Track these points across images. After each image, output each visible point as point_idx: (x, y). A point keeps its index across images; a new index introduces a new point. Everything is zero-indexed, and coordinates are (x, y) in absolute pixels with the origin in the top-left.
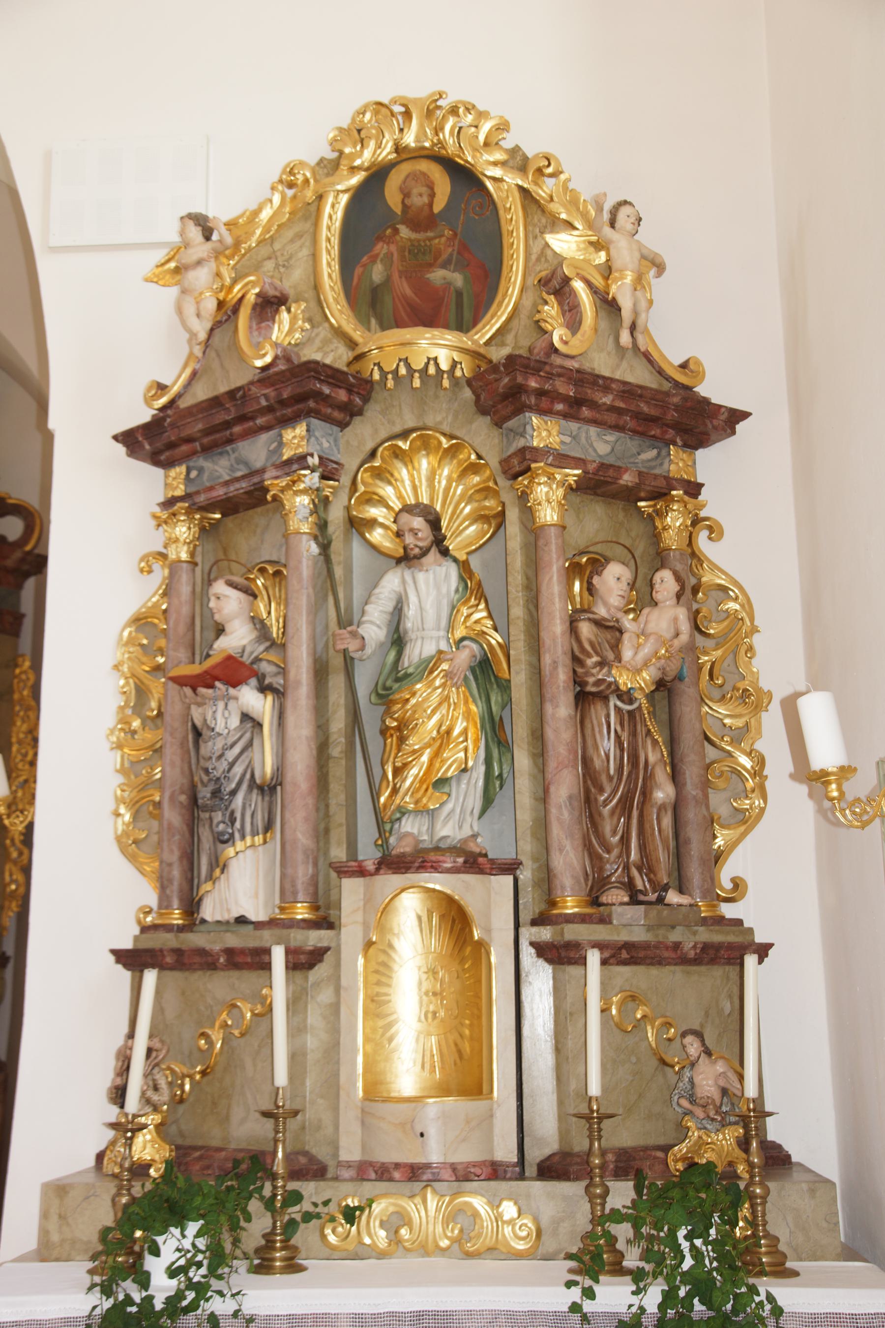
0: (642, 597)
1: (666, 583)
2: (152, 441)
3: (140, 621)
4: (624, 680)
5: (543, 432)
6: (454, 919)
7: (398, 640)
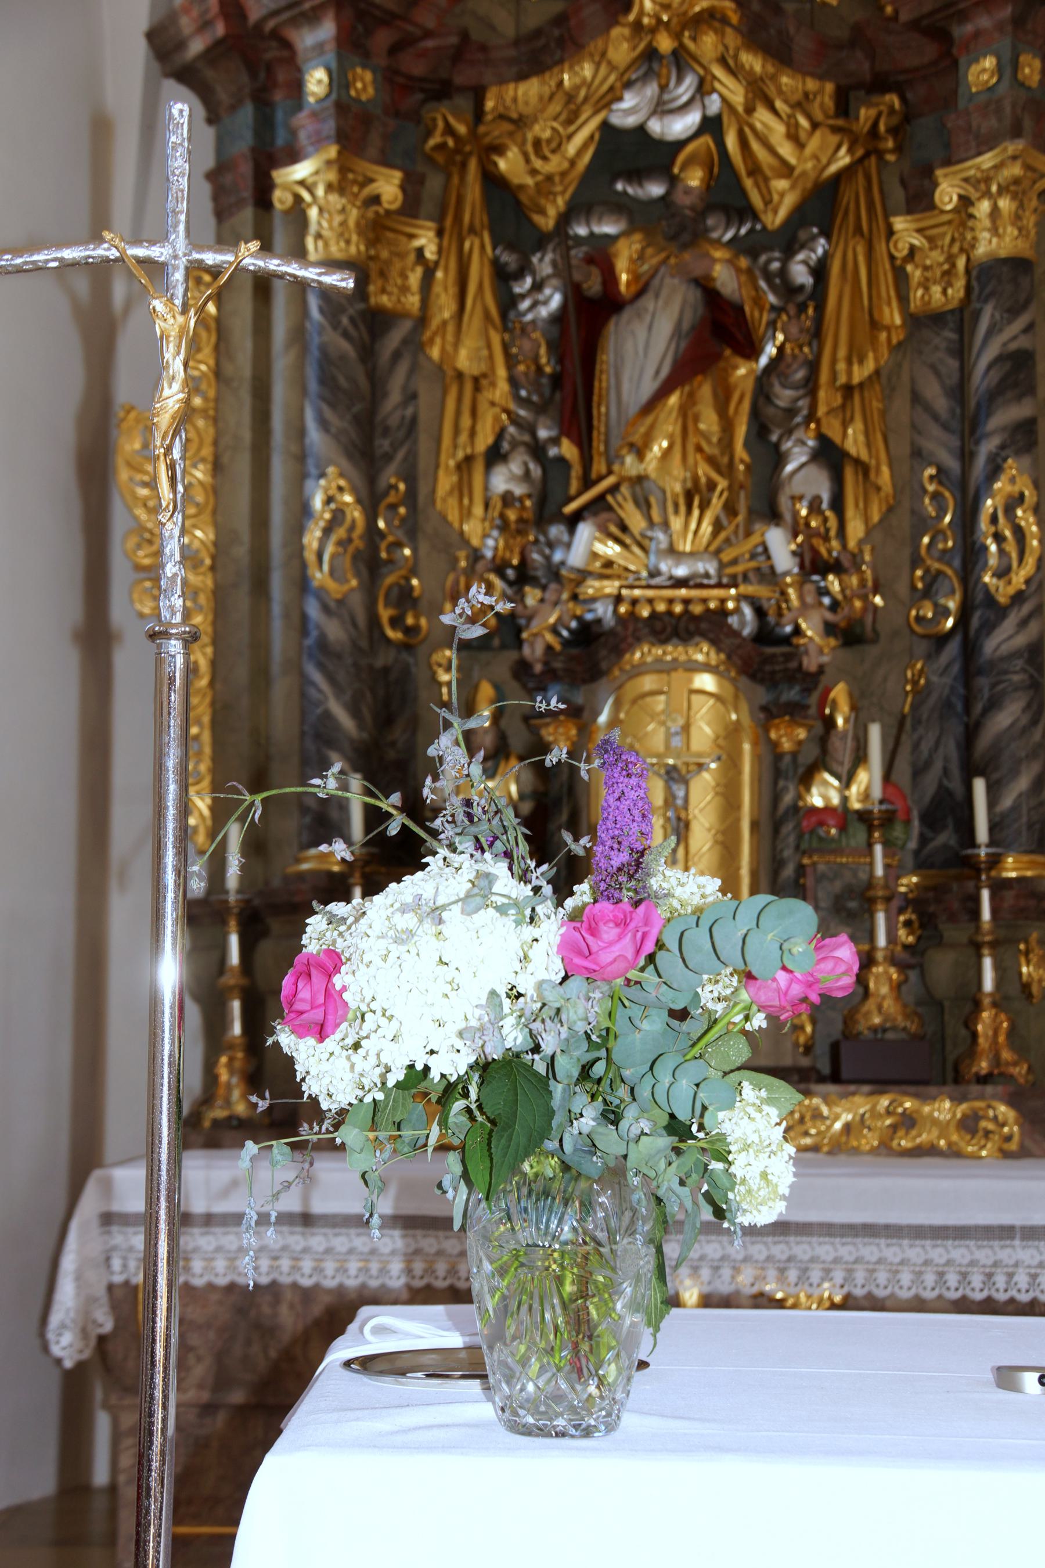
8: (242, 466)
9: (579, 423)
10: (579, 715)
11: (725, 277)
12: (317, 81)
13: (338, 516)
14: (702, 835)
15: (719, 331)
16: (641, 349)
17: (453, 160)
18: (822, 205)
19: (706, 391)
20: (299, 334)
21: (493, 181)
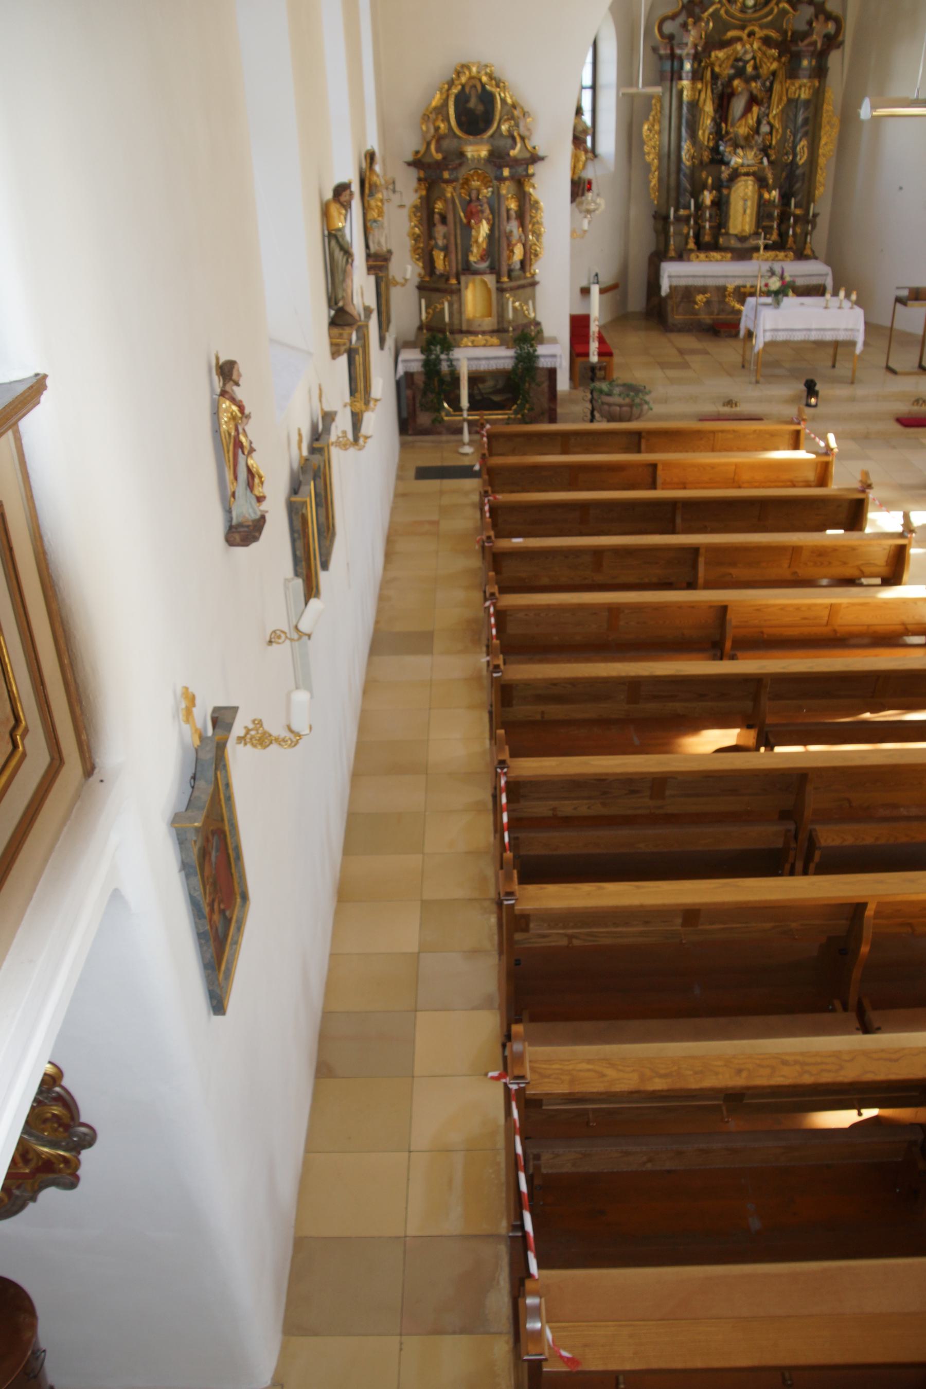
10: (729, 188)
11: (755, 92)
13: (689, 150)
15: (753, 100)
16: (738, 105)
17: (706, 68)
19: (749, 115)
21: (713, 71)
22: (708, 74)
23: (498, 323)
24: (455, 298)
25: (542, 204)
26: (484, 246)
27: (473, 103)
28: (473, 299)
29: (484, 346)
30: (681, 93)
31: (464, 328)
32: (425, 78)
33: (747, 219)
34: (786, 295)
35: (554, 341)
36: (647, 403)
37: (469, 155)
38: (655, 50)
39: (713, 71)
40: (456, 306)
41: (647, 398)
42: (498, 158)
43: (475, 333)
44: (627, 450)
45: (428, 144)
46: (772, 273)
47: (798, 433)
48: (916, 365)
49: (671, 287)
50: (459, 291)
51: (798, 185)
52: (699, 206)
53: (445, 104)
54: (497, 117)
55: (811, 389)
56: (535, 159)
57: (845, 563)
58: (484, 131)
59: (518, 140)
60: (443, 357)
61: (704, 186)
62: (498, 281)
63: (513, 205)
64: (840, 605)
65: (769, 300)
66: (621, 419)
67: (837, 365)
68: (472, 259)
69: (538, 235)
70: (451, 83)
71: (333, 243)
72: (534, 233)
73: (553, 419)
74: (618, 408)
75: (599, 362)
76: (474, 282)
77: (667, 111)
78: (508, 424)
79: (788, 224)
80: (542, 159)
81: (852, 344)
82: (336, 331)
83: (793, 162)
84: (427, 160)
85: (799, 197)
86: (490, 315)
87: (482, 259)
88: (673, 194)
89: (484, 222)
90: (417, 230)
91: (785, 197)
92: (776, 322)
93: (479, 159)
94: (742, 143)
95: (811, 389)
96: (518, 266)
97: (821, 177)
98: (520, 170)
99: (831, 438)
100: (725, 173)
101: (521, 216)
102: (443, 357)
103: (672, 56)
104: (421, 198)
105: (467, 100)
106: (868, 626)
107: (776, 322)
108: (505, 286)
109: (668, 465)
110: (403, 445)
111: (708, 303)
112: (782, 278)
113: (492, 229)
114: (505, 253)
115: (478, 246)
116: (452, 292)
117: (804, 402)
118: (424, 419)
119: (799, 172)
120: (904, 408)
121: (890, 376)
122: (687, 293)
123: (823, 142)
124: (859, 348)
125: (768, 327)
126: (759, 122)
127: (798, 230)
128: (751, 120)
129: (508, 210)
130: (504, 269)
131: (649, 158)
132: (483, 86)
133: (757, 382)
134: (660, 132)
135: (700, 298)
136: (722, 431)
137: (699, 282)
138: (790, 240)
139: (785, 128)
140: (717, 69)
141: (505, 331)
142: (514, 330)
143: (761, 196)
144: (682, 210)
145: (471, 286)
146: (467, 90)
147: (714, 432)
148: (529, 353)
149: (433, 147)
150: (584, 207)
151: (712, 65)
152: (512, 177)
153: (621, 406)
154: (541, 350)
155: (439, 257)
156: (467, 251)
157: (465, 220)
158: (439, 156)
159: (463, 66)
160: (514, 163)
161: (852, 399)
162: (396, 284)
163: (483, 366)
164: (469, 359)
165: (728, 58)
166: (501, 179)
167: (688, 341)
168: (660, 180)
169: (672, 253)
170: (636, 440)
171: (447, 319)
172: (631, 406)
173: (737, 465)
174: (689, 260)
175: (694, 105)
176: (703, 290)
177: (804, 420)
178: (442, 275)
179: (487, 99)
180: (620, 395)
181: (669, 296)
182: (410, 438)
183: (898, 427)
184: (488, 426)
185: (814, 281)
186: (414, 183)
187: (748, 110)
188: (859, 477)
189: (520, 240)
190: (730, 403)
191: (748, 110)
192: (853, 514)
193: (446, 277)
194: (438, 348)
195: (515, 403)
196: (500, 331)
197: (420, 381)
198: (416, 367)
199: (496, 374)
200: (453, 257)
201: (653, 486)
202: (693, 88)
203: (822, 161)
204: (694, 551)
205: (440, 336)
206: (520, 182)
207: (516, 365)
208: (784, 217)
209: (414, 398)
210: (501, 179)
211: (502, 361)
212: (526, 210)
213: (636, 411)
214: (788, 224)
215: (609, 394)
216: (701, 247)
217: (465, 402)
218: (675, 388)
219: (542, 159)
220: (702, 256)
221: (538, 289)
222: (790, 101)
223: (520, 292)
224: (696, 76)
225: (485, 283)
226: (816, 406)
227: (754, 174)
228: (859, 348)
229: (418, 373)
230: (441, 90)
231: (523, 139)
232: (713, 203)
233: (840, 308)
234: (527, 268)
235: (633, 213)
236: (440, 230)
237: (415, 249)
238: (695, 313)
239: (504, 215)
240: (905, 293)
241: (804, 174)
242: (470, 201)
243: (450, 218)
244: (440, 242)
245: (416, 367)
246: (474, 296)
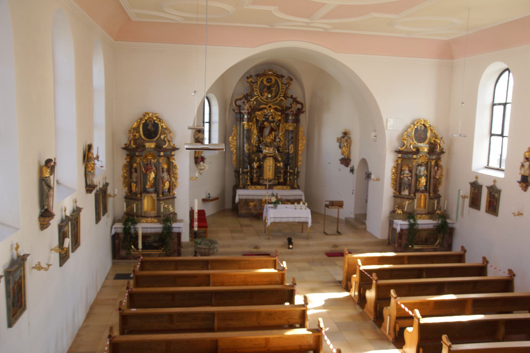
0: (438, 169)
1: (440, 169)
2: (398, 152)
3: (395, 167)
4: (437, 177)
5: (434, 157)
6: (425, 196)
7: (420, 172)
8: (238, 140)
9: (262, 136)
10: (263, 161)
11: (273, 127)
12: (246, 117)
14: (271, 170)
15: (272, 130)
16: (267, 131)
17: (253, 117)
18: (280, 120)
20: (244, 134)
21: (256, 119)
22: (255, 120)
23: (158, 213)
24: (139, 202)
25: (178, 167)
26: (152, 182)
27: (150, 127)
28: (147, 203)
29: (151, 223)
30: (244, 125)
31: (143, 215)
32: (130, 117)
33: (271, 173)
34: (279, 204)
35: (181, 221)
36: (215, 248)
37: (147, 146)
38: (234, 110)
39: (256, 119)
40: (139, 206)
41: (216, 246)
42: (159, 148)
43: (147, 217)
44: (203, 269)
45: (130, 141)
46: (273, 195)
47: (275, 260)
48: (336, 231)
49: (239, 199)
50: (141, 200)
51: (290, 161)
52: (252, 168)
53: (138, 126)
54: (159, 133)
55: (290, 242)
56: (175, 149)
57: (281, 318)
58: (154, 138)
59: (167, 142)
60: (132, 227)
61: (254, 161)
62: (158, 196)
63: (165, 167)
64: (269, 338)
65: (272, 205)
66: (205, 255)
67: (304, 231)
68: (147, 187)
69: (176, 179)
70: (141, 119)
71: (44, 183)
72: (174, 177)
73: (179, 255)
74: (203, 250)
75: (198, 230)
76: (148, 196)
77: (239, 132)
78: (159, 256)
79: (288, 174)
80: (178, 149)
81: (307, 223)
82: (42, 219)
83: (288, 153)
84: (130, 147)
85: (291, 166)
86: (154, 210)
87: (151, 187)
88: (242, 163)
89: (153, 173)
90: (125, 175)
91: (286, 165)
92: (274, 214)
93: (151, 148)
94: (269, 145)
95: (290, 242)
96: (167, 190)
97: (300, 158)
98: (168, 153)
99: (284, 263)
100: (261, 156)
101: (168, 171)
102: (132, 227)
103: (240, 113)
104: (128, 162)
105: (148, 125)
106: (284, 347)
107: (274, 214)
108: (160, 198)
109: (214, 275)
110: (114, 264)
111: (255, 206)
112: (277, 197)
113: (156, 176)
114: (161, 185)
115: (150, 182)
116: (138, 200)
117: (287, 247)
118: (123, 253)
119: (291, 156)
120: (328, 249)
121: (325, 236)
122: (246, 202)
123: (300, 145)
124: (310, 224)
125: (272, 216)
126: (275, 137)
127: (291, 178)
128: (272, 137)
129: (163, 169)
130: (161, 192)
131: (232, 149)
132: (154, 121)
133: (269, 239)
134: (236, 140)
135: (251, 204)
136: (244, 260)
137: (251, 198)
138: (288, 182)
139: (285, 140)
140: (258, 118)
141: (160, 217)
142: (164, 216)
143: (276, 165)
144: (245, 169)
145: (146, 198)
146: (148, 122)
147: (240, 261)
148: (169, 226)
149: (132, 143)
150: (199, 167)
151: (256, 116)
152: (164, 156)
153: (205, 249)
154: (174, 225)
155: (134, 186)
156: (145, 184)
157: (144, 172)
158: (134, 146)
159: (146, 113)
160: (166, 150)
161: (308, 246)
162: (110, 196)
163: (149, 231)
164: (142, 228)
165: (262, 114)
166: (160, 156)
167: (246, 221)
168: (237, 157)
169: (241, 186)
170: (206, 264)
171: (135, 211)
172: (209, 249)
173: (245, 275)
174: (248, 189)
175: (249, 131)
176: (253, 201)
177: (277, 255)
178: (135, 193)
179: (156, 126)
180: (204, 244)
181: (238, 203)
182: (117, 261)
183: (326, 257)
184: (142, 258)
185: (297, 198)
186: (125, 156)
187: (270, 133)
188: (291, 280)
189: (168, 180)
190: (256, 247)
191: (270, 133)
192: (290, 296)
193: (136, 194)
194: (130, 223)
195: (163, 247)
196: (157, 217)
197: (122, 236)
198: (120, 231)
199: (155, 234)
200: (139, 186)
201: (208, 285)
202: (248, 125)
203: (300, 152)
204: (213, 314)
205: (132, 218)
206: (169, 158)
207: (163, 232)
208: (286, 173)
209: (119, 244)
210: (160, 156)
211: (157, 229)
212: (171, 169)
213: (211, 251)
214: (288, 174)
215: (200, 244)
216: (253, 183)
217: (140, 246)
218: (229, 242)
219: (178, 149)
220: (253, 187)
221: (176, 199)
222: (286, 130)
223: (167, 201)
224: (249, 120)
225: (152, 197)
226: (292, 248)
227: (272, 156)
228: (310, 224)
229: (122, 233)
230: (137, 121)
231: (169, 141)
232: (257, 167)
233: (301, 209)
234: (171, 191)
235: (227, 169)
236: (134, 175)
237: (124, 182)
238: (250, 210)
239: (161, 170)
240: (328, 203)
241: (292, 157)
242: (147, 164)
243: (138, 170)
244: (134, 180)
245: (120, 231)
246: (148, 202)
